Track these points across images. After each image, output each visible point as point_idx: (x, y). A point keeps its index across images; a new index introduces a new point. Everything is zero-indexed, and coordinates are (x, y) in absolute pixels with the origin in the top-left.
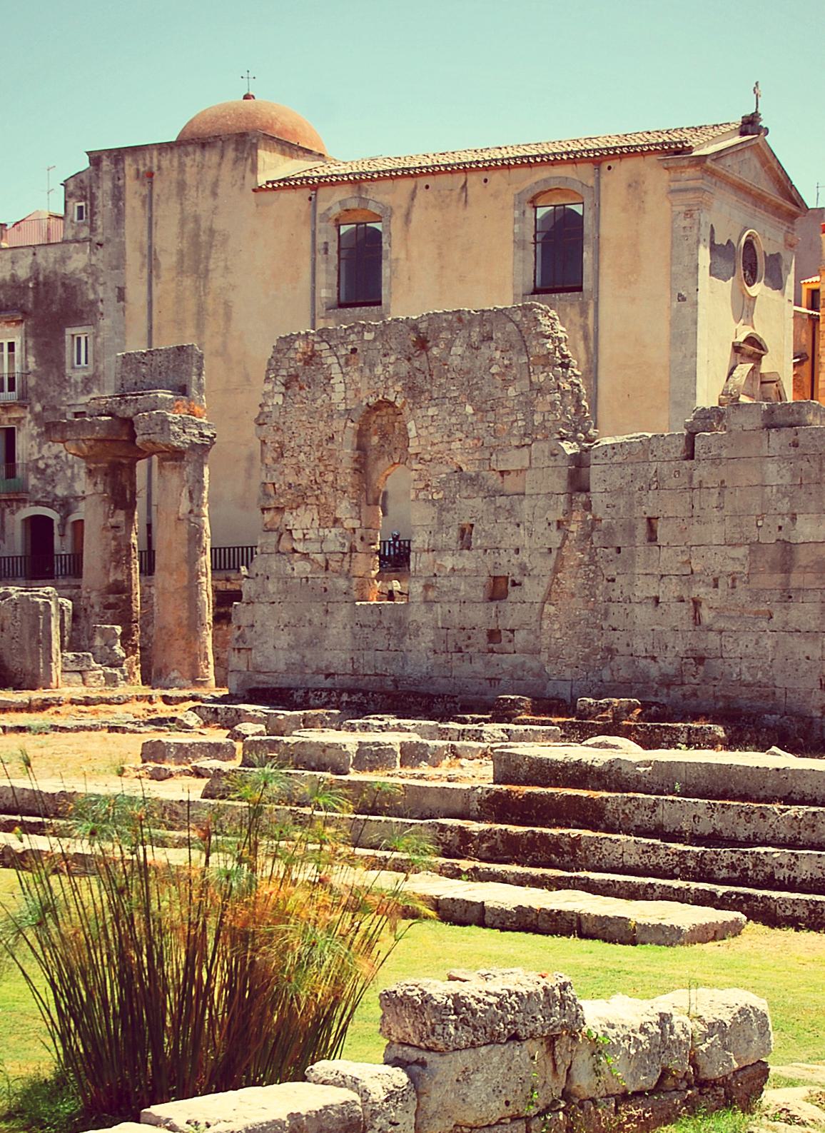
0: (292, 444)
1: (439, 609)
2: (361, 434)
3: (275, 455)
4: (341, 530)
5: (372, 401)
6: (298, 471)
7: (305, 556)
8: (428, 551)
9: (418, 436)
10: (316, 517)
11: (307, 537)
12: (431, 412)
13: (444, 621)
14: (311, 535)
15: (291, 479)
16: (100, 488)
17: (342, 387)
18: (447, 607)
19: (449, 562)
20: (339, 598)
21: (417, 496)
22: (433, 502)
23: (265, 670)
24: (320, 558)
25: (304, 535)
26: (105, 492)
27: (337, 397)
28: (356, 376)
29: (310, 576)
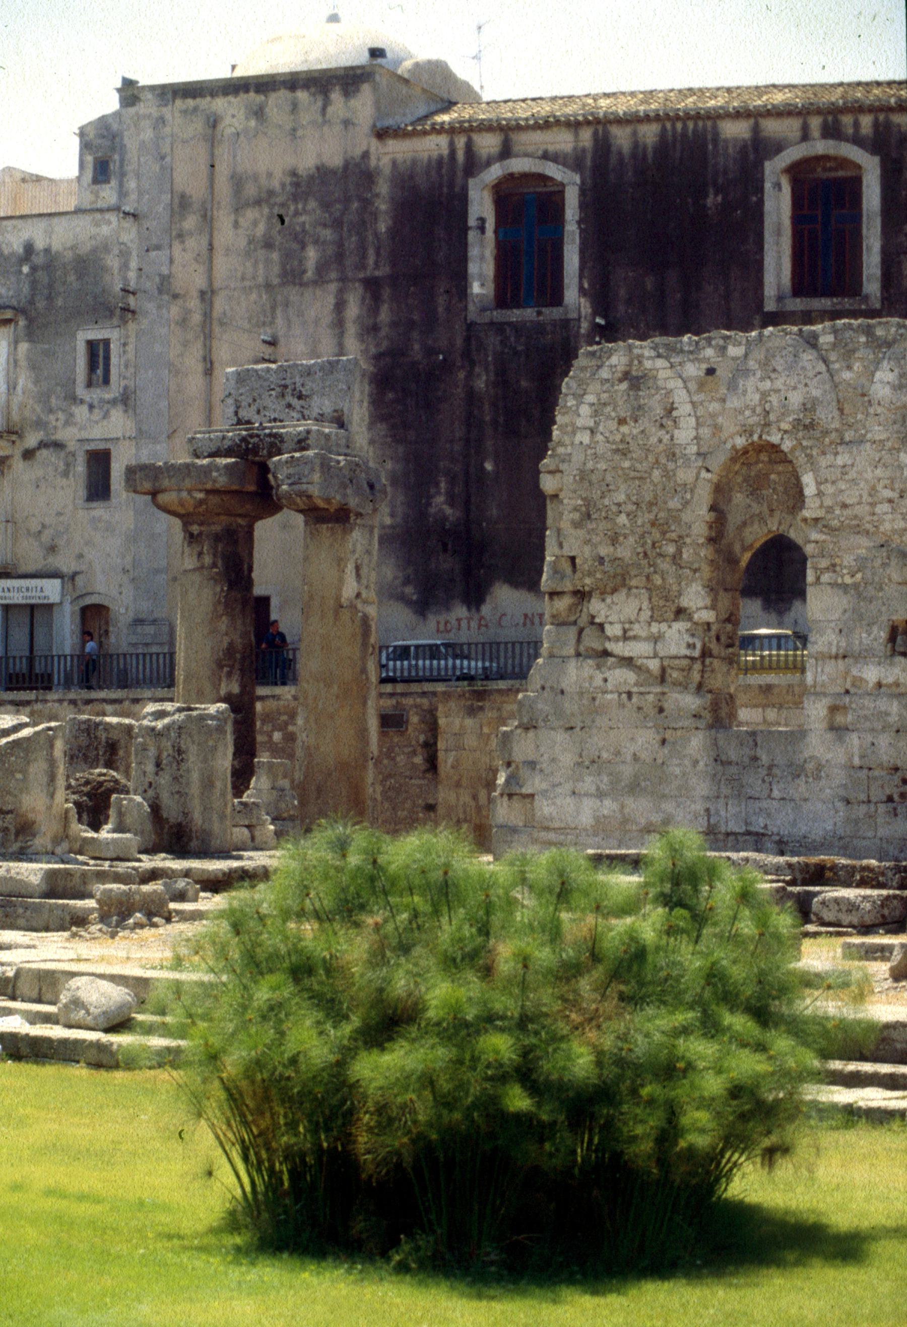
0: (606, 502)
1: (856, 742)
2: (718, 489)
3: (576, 516)
4: (689, 625)
5: (740, 442)
6: (614, 540)
7: (628, 662)
8: (836, 657)
9: (820, 494)
10: (645, 605)
11: (631, 633)
12: (840, 461)
13: (862, 757)
14: (637, 630)
15: (604, 551)
16: (207, 560)
17: (692, 422)
18: (870, 739)
19: (871, 674)
20: (686, 723)
21: (818, 578)
22: (845, 587)
23: (557, 825)
24: (654, 665)
25: (625, 631)
26: (214, 565)
27: (685, 434)
28: (714, 407)
29: (635, 689)
